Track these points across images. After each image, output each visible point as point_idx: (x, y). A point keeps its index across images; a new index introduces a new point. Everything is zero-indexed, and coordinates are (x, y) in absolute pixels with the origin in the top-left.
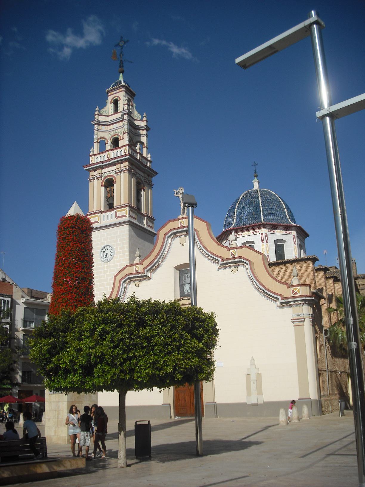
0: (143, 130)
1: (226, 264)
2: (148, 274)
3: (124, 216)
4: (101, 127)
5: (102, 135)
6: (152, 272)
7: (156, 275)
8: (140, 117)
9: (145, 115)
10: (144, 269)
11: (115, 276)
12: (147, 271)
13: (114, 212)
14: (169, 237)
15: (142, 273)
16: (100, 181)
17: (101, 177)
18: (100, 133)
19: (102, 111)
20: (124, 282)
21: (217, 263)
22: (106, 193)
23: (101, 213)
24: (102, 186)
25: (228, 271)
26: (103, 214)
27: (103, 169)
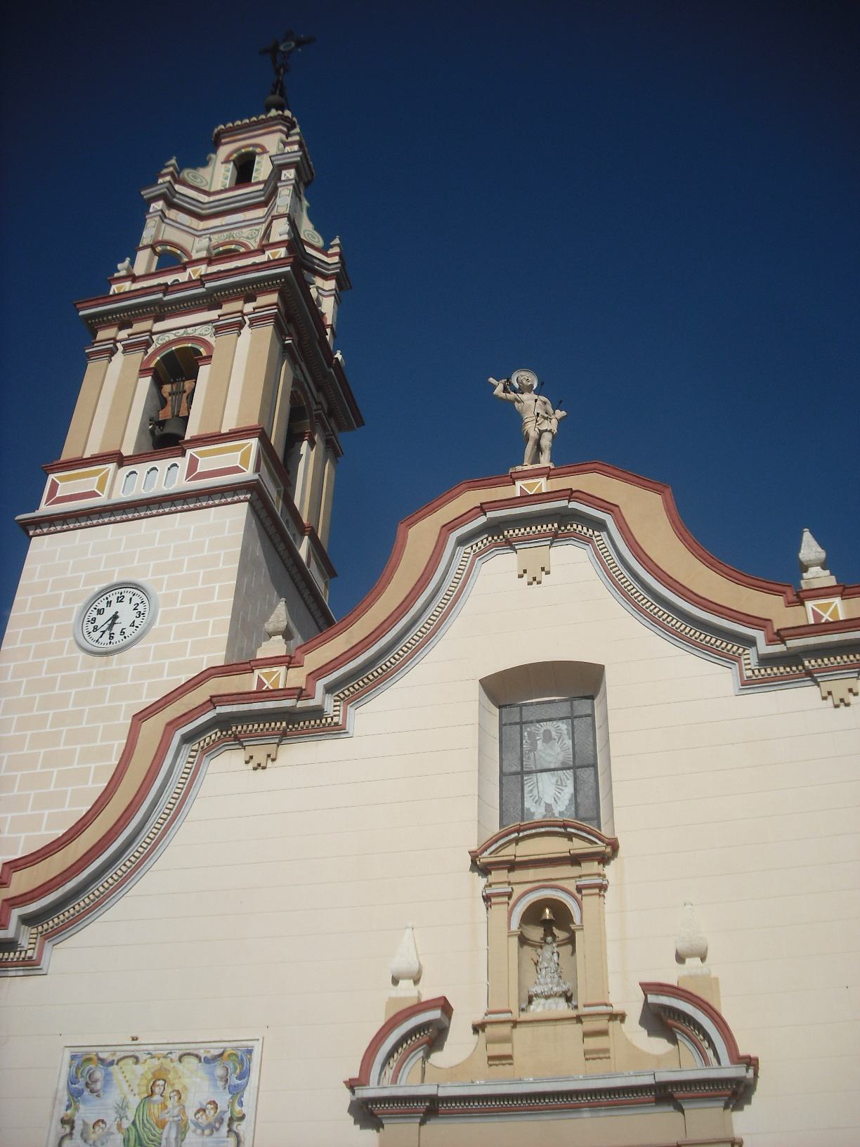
0: (326, 277)
1: (792, 658)
2: (329, 705)
3: (236, 470)
4: (172, 214)
5: (170, 234)
6: (355, 699)
7: (371, 717)
8: (318, 241)
9: (337, 241)
10: (316, 675)
11: (141, 717)
12: (329, 689)
13: (183, 462)
14: (462, 541)
15: (300, 693)
16: (137, 357)
17: (148, 344)
18: (169, 229)
19: (187, 174)
20: (187, 739)
21: (735, 659)
22: (158, 399)
23: (121, 460)
24: (143, 372)
25: (801, 699)
26: (126, 470)
27: (158, 319)
